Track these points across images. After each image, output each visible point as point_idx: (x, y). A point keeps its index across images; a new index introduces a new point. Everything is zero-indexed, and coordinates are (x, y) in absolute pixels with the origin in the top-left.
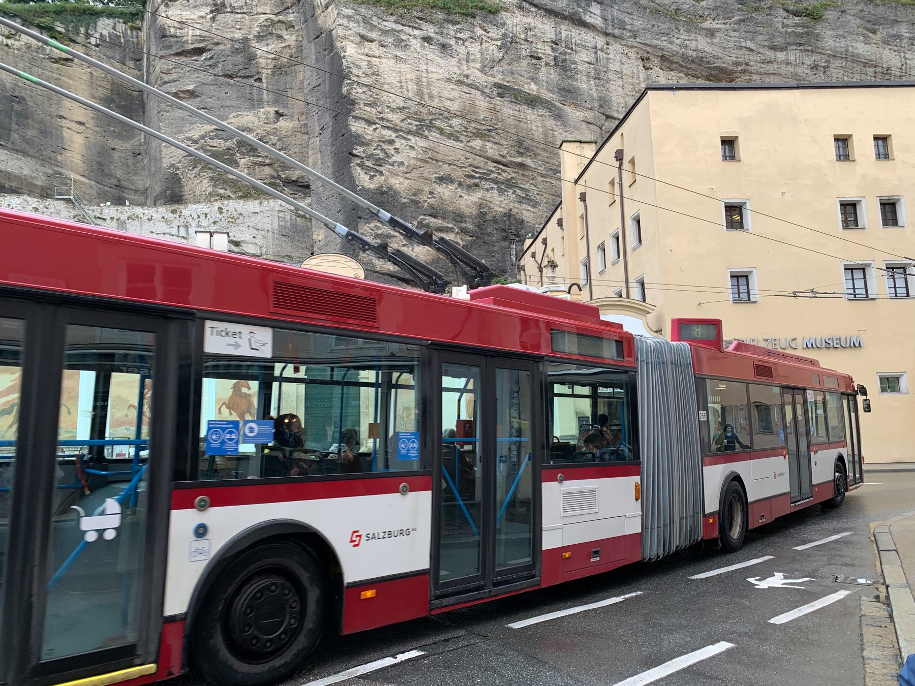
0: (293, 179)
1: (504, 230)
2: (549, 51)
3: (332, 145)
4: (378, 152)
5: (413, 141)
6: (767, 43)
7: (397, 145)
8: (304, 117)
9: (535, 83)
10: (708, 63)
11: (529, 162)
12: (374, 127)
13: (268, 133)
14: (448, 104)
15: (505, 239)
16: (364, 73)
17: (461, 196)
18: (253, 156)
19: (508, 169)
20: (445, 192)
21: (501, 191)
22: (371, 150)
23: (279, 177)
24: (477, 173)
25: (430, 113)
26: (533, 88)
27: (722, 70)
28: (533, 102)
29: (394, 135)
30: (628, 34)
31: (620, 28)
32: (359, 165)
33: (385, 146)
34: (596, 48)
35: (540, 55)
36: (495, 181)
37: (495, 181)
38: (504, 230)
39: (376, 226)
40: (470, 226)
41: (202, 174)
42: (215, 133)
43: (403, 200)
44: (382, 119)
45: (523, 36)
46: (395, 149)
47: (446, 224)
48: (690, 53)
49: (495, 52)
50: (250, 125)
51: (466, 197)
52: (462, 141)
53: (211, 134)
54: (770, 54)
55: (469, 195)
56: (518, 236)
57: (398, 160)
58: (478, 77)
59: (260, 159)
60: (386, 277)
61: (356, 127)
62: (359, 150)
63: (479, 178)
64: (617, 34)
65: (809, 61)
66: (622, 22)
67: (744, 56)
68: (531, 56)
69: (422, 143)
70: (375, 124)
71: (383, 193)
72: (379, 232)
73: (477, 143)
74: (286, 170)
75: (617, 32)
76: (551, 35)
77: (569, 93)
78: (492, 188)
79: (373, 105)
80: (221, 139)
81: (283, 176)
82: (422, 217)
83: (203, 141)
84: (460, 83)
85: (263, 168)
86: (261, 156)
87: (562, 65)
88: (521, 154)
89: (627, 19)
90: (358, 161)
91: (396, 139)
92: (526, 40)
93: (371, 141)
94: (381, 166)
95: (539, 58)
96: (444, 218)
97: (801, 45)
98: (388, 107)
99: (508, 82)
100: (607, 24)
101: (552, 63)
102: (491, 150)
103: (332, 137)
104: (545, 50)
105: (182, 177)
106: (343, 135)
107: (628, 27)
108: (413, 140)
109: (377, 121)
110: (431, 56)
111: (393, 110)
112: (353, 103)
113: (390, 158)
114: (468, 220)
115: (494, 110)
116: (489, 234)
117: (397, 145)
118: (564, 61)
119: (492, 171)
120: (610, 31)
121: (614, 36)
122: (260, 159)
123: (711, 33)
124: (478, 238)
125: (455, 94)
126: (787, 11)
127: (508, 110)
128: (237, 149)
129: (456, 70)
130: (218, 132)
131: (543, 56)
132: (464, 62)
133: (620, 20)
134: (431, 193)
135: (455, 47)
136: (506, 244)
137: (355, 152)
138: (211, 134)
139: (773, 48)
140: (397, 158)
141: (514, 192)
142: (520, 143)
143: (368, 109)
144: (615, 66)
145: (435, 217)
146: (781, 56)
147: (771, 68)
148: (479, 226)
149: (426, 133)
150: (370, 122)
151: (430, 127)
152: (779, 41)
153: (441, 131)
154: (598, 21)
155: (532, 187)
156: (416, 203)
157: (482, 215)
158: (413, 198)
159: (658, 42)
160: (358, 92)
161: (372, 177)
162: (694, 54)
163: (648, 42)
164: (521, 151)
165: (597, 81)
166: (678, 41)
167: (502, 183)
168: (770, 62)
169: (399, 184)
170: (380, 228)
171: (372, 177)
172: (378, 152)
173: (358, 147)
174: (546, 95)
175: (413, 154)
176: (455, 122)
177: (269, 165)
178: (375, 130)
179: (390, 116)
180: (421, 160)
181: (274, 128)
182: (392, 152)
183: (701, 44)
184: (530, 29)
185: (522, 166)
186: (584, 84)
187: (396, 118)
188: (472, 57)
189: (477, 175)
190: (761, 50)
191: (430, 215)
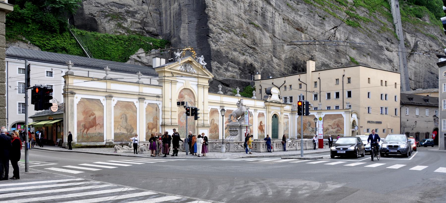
0: (151, 31)
1: (250, 70)
2: (260, 11)
3: (196, 29)
4: (217, 37)
5: (227, 35)
6: (313, 23)
7: (222, 35)
8: (154, 6)
9: (257, 21)
10: (298, 25)
11: (256, 48)
12: (215, 27)
13: (139, 10)
14: (235, 23)
15: (250, 73)
16: (212, 7)
17: (240, 57)
18: (134, 18)
19: (251, 49)
20: (235, 54)
21: (250, 56)
22: (214, 35)
23: (145, 30)
24: (244, 49)
25: (231, 26)
26: (256, 22)
27: (301, 28)
28: (257, 27)
29: (221, 32)
30: (281, 10)
31: (279, 8)
32: (211, 40)
33: (219, 35)
34: (273, 13)
35: (258, 11)
36: (248, 53)
37: (248, 53)
38: (250, 70)
39: (216, 64)
40: (241, 67)
41: (111, 22)
42: (113, 4)
43: (224, 55)
44: (218, 25)
45: (254, 4)
46: (222, 37)
47: (235, 66)
48: (295, 20)
49: (247, 7)
50: (131, 4)
51: (241, 57)
52: (239, 37)
53: (111, 4)
54: (313, 26)
55: (242, 57)
56: (253, 72)
57: (223, 41)
58: (243, 16)
59: (136, 20)
60: (218, 82)
61: (211, 26)
62: (211, 35)
63: (244, 51)
64: (278, 10)
65: (321, 31)
66: (280, 6)
67: (307, 25)
68: (256, 11)
69: (229, 36)
70: (216, 26)
71: (218, 52)
72: (217, 66)
73: (243, 39)
74: (147, 27)
75: (278, 9)
76: (261, 5)
77: (265, 26)
78: (248, 55)
79: (215, 19)
80: (116, 7)
81: (146, 29)
82: (229, 62)
83: (107, 6)
84: (239, 16)
85: (137, 24)
86: (137, 19)
87: (263, 16)
88: (254, 45)
89: (281, 6)
90: (211, 39)
91: (222, 33)
92: (255, 5)
93: (214, 32)
94: (218, 42)
95: (257, 12)
96: (234, 63)
97: (321, 26)
98: (219, 21)
99: (251, 19)
100: (276, 6)
101: (261, 15)
102: (248, 42)
103: (196, 26)
104: (259, 10)
105: (97, 21)
106: (204, 28)
107: (281, 8)
108: (227, 34)
109: (216, 25)
110: (231, 5)
111: (220, 22)
112: (209, 17)
113: (220, 40)
114: (241, 65)
115: (248, 28)
116: (246, 71)
117: (222, 35)
118: (264, 15)
119: (248, 50)
120: (276, 8)
121: (277, 10)
122: (136, 20)
123: (301, 16)
124: (243, 71)
125: (237, 20)
126: (318, 15)
127: (252, 28)
128: (125, 14)
129: (237, 11)
130: (114, 3)
131: (259, 12)
132: (239, 9)
133: (279, 5)
134: (232, 54)
135: (237, 3)
136: (250, 74)
137: (210, 35)
138: (111, 4)
139: (314, 25)
140: (223, 40)
141: (253, 58)
142: (254, 40)
143: (214, 20)
144: (277, 20)
145: (232, 63)
146: (316, 28)
147: (313, 31)
148: (244, 68)
149: (230, 32)
150: (214, 26)
151: (232, 31)
152: (316, 23)
153: (235, 34)
154: (274, 4)
155: (257, 57)
156: (227, 57)
157: (245, 64)
158: (227, 55)
159: (288, 15)
160: (210, 14)
161: (216, 46)
162: (296, 21)
163: (285, 14)
164: (255, 44)
165: (272, 24)
166: (293, 16)
167: (250, 54)
168: (313, 29)
169: (223, 50)
170: (217, 65)
171: (216, 46)
172: (217, 37)
173: (211, 34)
174: (260, 26)
175: (227, 39)
176: (238, 30)
177: (140, 23)
178: (216, 28)
179: (220, 24)
180: (229, 42)
181: (142, 8)
182: (221, 38)
183: (298, 18)
184: (257, 2)
185: (254, 48)
186: (269, 24)
187: (221, 25)
188: (241, 8)
189: (244, 50)
190: (311, 25)
191: (231, 62)
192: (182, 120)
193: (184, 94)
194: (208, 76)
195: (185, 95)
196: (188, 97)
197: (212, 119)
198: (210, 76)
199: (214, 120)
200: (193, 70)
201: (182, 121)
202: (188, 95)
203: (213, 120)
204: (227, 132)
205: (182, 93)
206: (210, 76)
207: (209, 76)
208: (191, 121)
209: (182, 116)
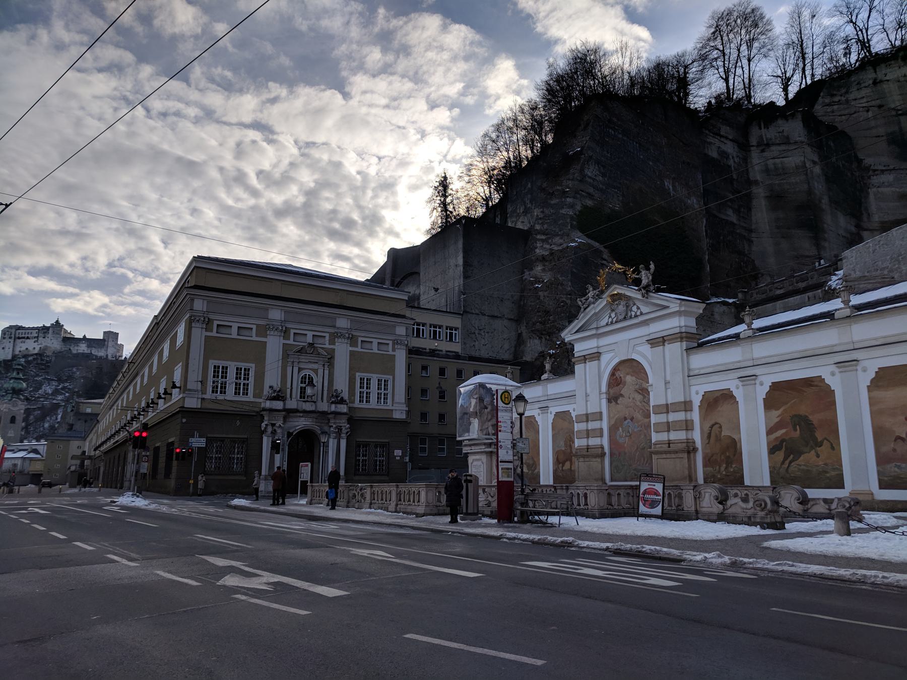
192: (621, 437)
193: (621, 375)
194: (666, 307)
195: (625, 377)
196: (634, 378)
197: (713, 422)
198: (671, 305)
199: (721, 427)
200: (638, 308)
201: (621, 441)
202: (632, 376)
203: (717, 426)
204: (783, 463)
205: (618, 374)
206: (671, 305)
207: (666, 307)
208: (643, 437)
209: (620, 429)
